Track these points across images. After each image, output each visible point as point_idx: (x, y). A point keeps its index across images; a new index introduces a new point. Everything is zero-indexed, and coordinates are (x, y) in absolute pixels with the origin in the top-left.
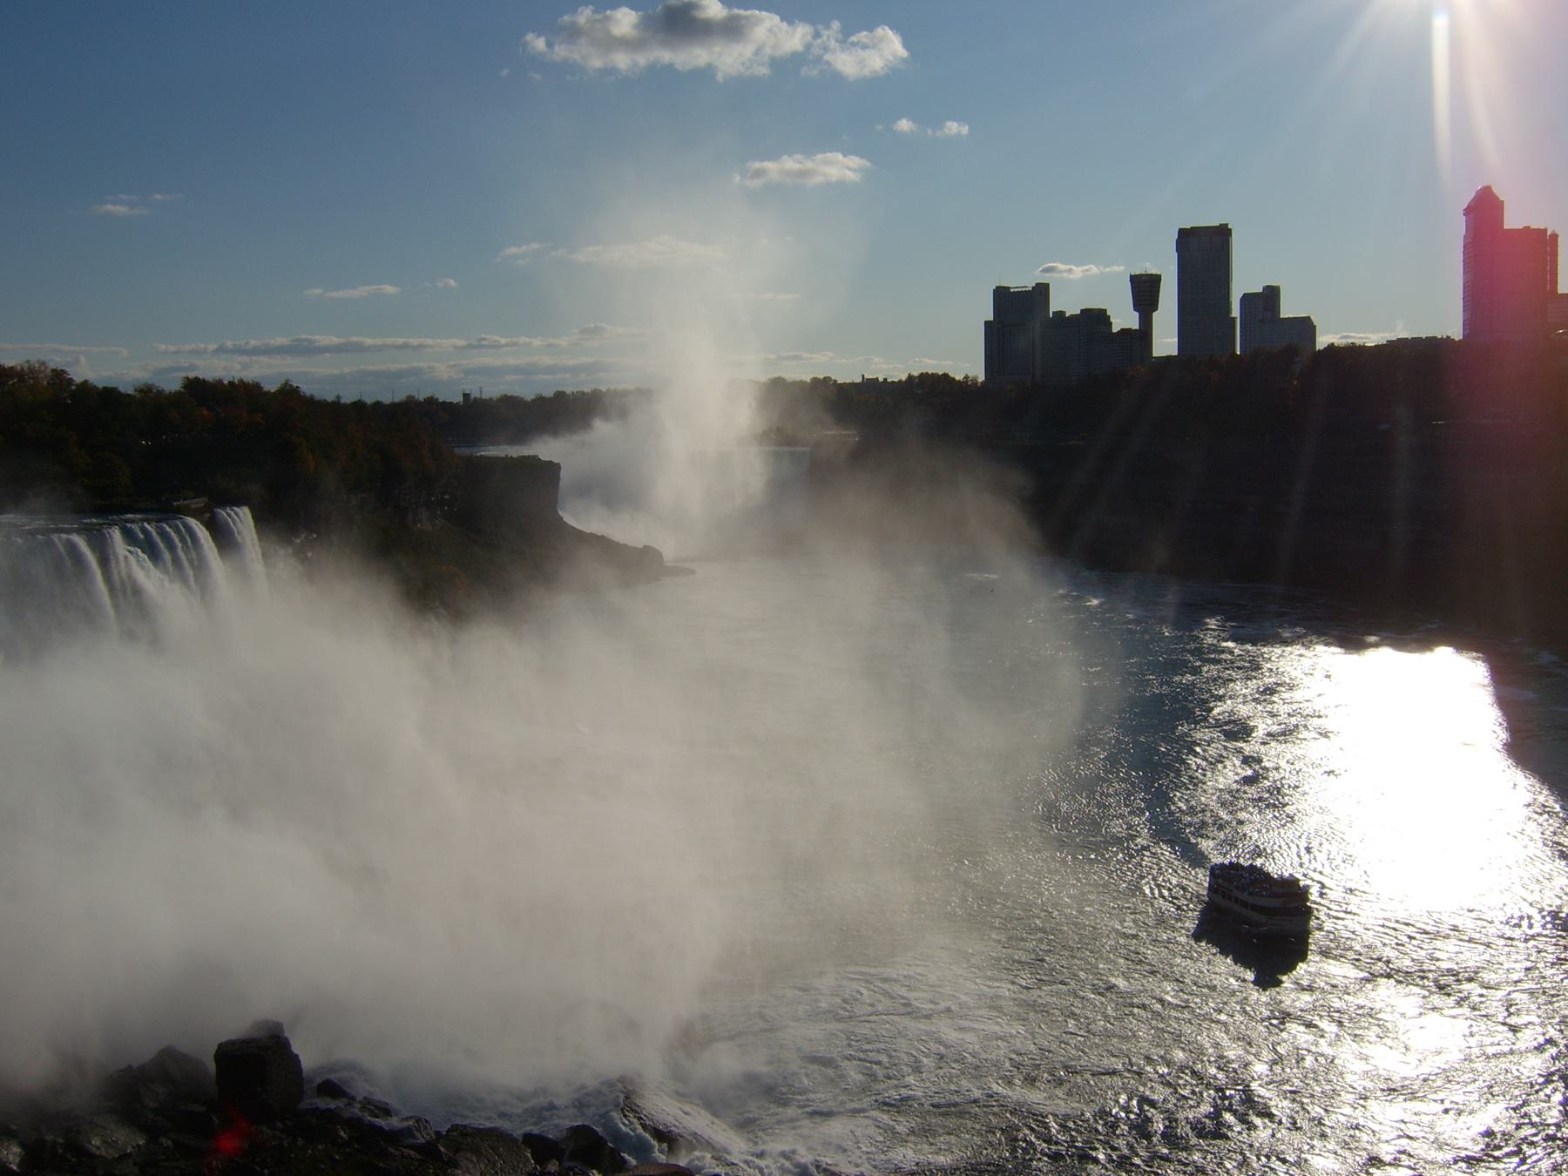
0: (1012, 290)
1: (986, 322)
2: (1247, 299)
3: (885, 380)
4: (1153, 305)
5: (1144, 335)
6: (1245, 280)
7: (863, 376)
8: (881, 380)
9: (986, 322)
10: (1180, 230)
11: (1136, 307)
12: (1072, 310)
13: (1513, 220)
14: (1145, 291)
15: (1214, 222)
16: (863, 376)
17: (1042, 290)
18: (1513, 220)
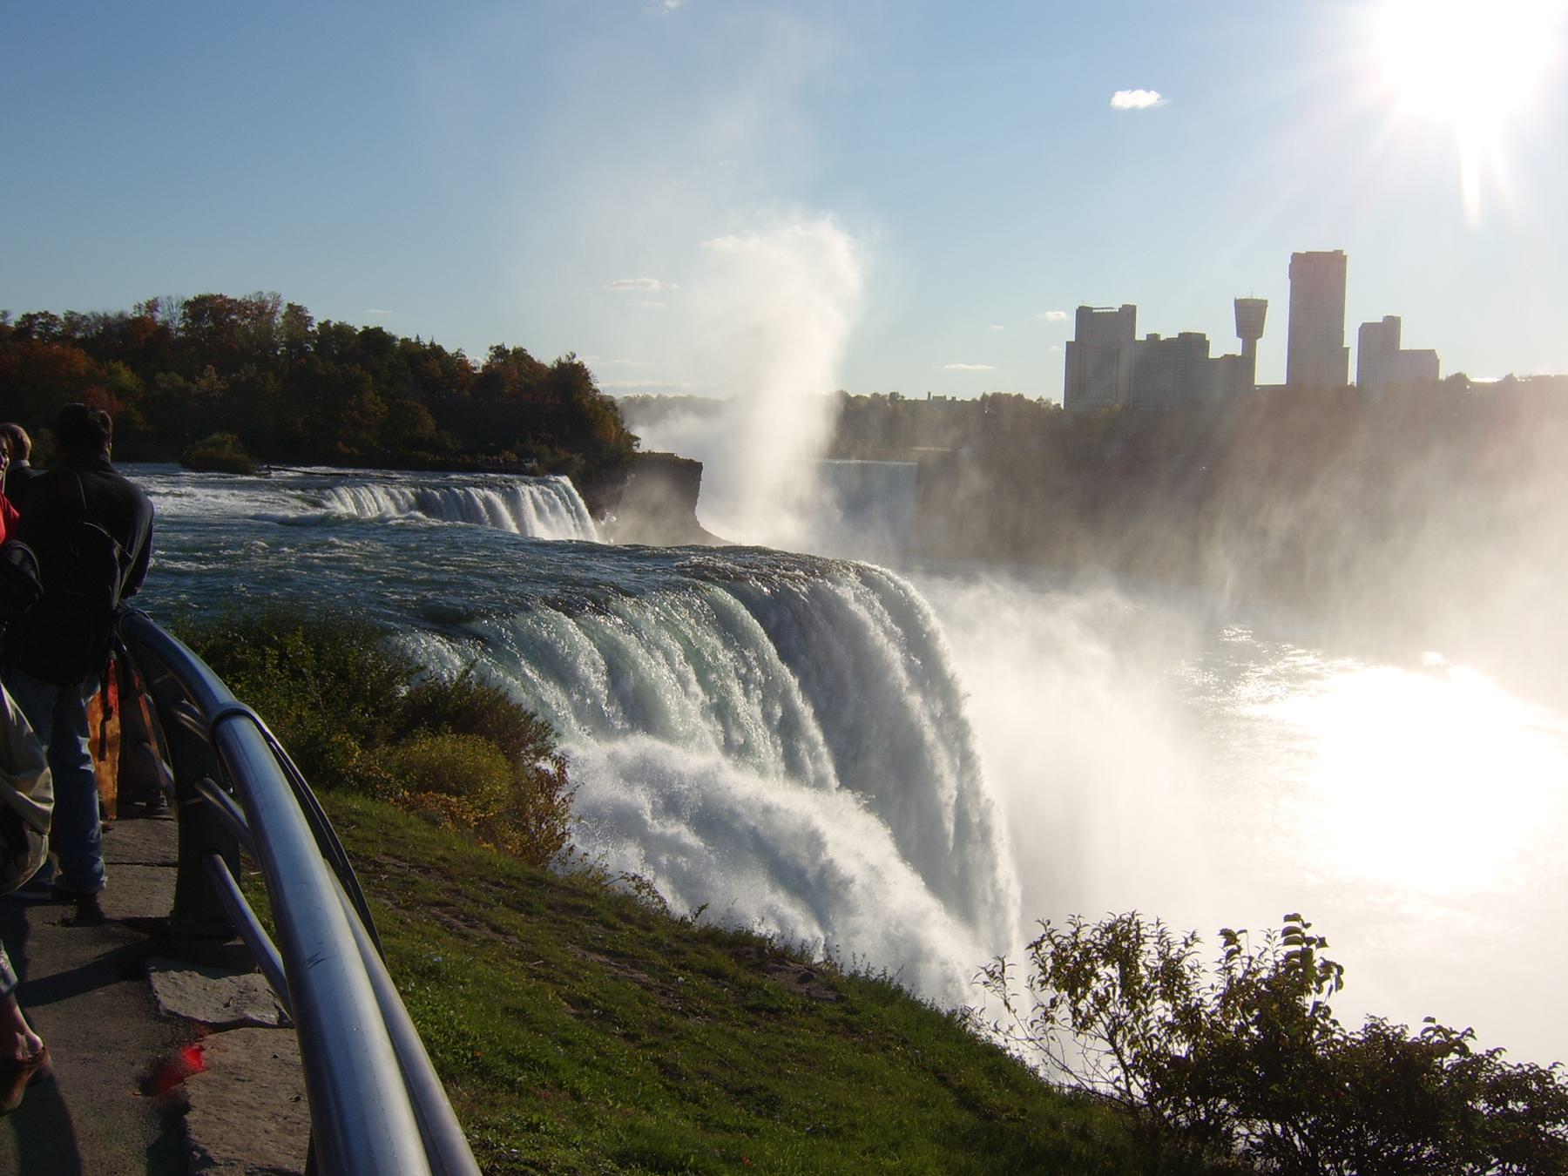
0: (1094, 311)
1: (1068, 343)
2: (1366, 330)
3: (954, 398)
4: (1258, 332)
5: (1244, 364)
6: (1359, 310)
7: (929, 394)
8: (949, 398)
9: (1068, 343)
10: (1294, 254)
11: (1239, 334)
12: (1168, 332)
14: (1250, 318)
16: (929, 394)
17: (1129, 313)
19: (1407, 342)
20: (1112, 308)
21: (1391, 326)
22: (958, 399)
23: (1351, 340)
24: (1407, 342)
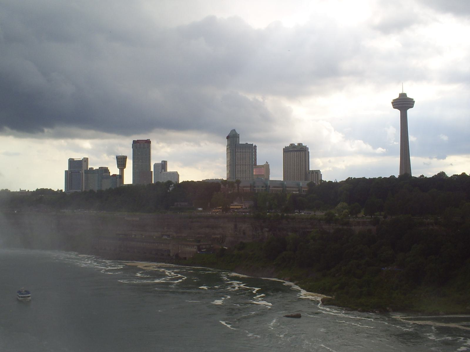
0: (75, 160)
2: (156, 165)
3: (28, 191)
7: (20, 189)
8: (27, 191)
9: (65, 171)
12: (96, 167)
13: (242, 141)
14: (121, 162)
15: (146, 139)
16: (20, 189)
17: (86, 160)
18: (242, 141)
19: (170, 169)
20: (80, 159)
21: (164, 165)
22: (30, 191)
23: (152, 169)
24: (170, 169)
